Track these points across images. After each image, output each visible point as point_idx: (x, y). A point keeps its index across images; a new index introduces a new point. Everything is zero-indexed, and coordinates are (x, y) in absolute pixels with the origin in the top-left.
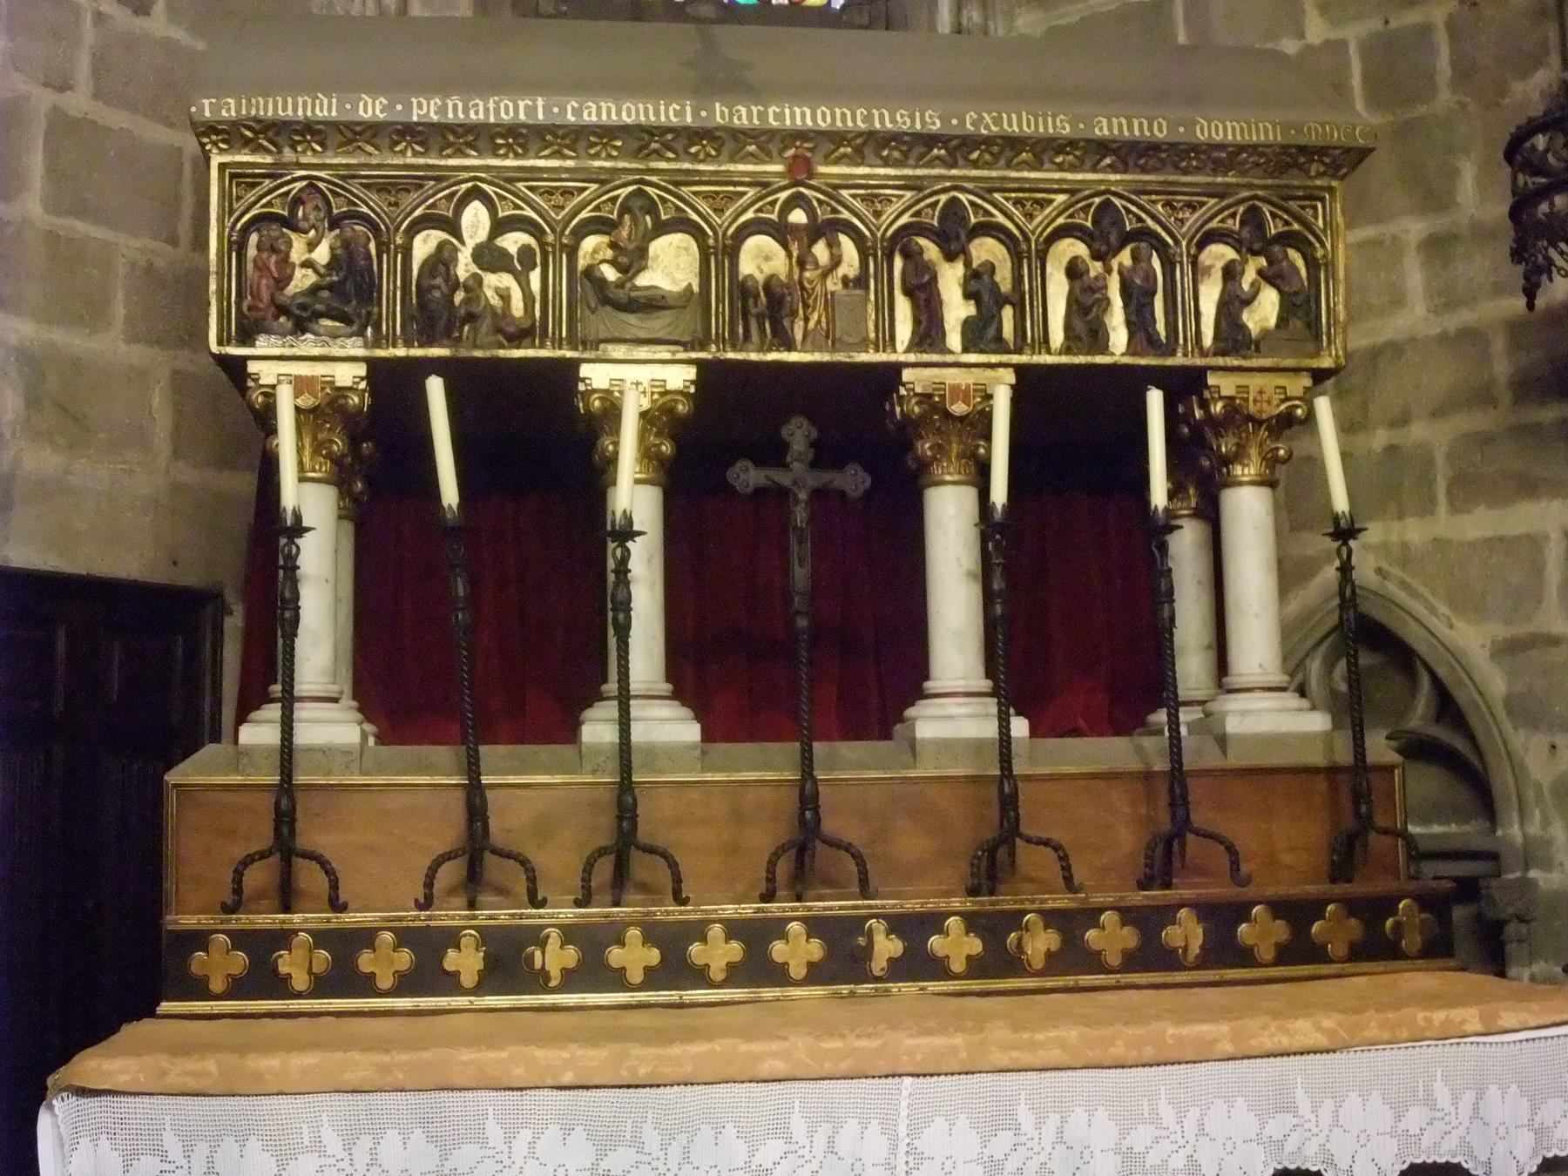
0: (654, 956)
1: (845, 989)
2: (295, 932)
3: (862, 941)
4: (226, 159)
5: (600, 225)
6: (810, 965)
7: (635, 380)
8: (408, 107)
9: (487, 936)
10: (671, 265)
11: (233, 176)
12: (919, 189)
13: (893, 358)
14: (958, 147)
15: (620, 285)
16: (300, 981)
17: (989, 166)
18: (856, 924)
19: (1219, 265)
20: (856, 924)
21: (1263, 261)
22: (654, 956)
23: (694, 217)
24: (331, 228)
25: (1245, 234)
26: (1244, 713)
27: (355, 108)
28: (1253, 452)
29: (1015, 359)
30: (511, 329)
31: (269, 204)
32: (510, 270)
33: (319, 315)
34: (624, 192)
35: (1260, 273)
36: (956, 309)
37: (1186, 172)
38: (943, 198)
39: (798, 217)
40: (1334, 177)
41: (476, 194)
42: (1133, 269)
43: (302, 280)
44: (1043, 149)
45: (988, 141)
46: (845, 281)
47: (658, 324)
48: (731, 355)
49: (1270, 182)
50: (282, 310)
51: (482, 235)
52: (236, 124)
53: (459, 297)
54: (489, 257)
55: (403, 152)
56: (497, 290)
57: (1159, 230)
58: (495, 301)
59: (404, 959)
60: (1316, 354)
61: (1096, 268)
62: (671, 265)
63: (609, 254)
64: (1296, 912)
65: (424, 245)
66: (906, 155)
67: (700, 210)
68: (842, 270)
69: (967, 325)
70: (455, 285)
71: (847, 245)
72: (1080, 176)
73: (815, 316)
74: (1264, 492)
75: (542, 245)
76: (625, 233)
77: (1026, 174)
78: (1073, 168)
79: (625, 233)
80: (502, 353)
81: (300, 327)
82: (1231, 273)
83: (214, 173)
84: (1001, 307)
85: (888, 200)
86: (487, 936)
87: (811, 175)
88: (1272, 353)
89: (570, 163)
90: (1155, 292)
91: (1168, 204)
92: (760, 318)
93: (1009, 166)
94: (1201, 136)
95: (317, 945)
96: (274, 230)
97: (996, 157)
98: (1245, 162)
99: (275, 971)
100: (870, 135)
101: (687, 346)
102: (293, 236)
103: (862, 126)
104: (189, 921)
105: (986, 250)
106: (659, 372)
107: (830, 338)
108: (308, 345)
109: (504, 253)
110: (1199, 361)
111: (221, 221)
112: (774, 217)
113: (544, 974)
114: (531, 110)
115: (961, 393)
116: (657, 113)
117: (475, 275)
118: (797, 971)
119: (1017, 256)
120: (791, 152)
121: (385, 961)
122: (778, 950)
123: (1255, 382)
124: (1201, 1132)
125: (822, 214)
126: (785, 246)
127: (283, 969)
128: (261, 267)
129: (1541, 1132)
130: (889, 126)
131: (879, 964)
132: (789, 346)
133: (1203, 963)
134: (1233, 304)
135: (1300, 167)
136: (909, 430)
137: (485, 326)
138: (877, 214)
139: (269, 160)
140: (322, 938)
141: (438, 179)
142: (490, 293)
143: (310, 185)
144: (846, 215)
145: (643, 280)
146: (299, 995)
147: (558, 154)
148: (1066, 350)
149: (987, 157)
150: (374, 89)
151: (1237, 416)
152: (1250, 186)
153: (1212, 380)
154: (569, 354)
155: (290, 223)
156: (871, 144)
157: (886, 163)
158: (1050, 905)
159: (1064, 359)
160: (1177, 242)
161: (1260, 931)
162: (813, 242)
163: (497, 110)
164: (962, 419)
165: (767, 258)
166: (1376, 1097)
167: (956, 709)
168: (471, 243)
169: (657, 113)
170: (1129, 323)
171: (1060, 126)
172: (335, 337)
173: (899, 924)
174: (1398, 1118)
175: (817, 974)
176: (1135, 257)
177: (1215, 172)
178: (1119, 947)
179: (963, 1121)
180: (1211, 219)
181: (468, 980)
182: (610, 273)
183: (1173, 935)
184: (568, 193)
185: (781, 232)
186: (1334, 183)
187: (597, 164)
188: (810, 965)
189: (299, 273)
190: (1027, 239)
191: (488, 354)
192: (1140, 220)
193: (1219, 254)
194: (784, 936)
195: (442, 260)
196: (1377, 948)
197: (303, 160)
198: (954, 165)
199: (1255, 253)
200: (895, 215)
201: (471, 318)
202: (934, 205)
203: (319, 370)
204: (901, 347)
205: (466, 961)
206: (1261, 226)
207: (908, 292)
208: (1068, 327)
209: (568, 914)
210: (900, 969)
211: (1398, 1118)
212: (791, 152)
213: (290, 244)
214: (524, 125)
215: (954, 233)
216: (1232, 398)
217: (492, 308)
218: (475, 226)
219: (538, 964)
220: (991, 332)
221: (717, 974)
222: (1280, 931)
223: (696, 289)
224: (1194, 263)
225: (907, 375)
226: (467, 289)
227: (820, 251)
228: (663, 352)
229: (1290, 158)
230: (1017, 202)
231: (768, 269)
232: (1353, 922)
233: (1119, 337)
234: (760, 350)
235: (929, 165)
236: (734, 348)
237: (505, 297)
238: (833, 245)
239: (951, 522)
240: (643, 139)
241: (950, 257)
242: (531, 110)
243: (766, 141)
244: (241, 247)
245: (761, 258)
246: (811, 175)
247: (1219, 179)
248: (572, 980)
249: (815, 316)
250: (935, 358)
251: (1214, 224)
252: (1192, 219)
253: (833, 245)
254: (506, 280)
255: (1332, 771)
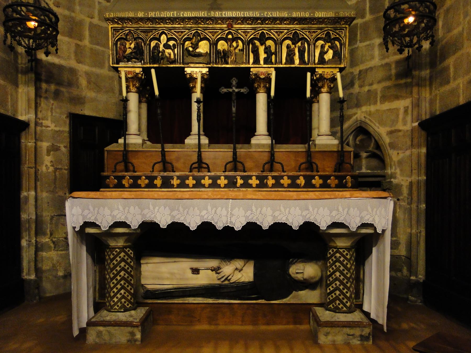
0: (194, 182)
1: (231, 189)
2: (126, 176)
3: (235, 180)
4: (112, 26)
5: (188, 39)
6: (225, 184)
7: (197, 71)
8: (148, 14)
9: (163, 177)
10: (203, 47)
11: (114, 30)
12: (255, 30)
13: (248, 66)
14: (263, 20)
15: (193, 51)
16: (127, 185)
17: (270, 24)
18: (235, 177)
19: (320, 45)
20: (235, 177)
21: (330, 44)
22: (194, 182)
23: (208, 37)
24: (134, 40)
25: (326, 38)
26: (320, 140)
27: (137, 14)
28: (326, 86)
29: (274, 66)
30: (170, 61)
31: (121, 35)
32: (171, 49)
33: (132, 58)
34: (193, 32)
35: (329, 46)
36: (262, 56)
37: (313, 24)
38: (260, 32)
39: (230, 37)
40: (347, 25)
41: (163, 33)
42: (300, 47)
43: (129, 51)
44: (282, 20)
45: (270, 18)
46: (239, 50)
47: (200, 59)
48: (215, 66)
49: (332, 26)
50: (125, 57)
51: (165, 42)
52: (113, 18)
53: (160, 54)
54: (167, 46)
55: (148, 24)
56: (168, 53)
57: (307, 38)
58: (168, 55)
59: (147, 181)
60: (340, 64)
61: (293, 46)
62: (203, 47)
63: (191, 45)
64: (325, 178)
65: (153, 44)
66: (252, 22)
67: (209, 36)
68: (239, 48)
69: (265, 59)
70: (159, 52)
71: (240, 42)
72: (290, 26)
73: (232, 58)
74: (328, 95)
75: (177, 43)
76: (194, 40)
77: (278, 26)
78: (288, 24)
79: (194, 40)
80: (169, 66)
81: (128, 61)
82: (323, 47)
83: (110, 29)
84: (272, 55)
85: (248, 32)
86: (163, 177)
87: (232, 27)
88: (331, 64)
89: (182, 26)
90: (305, 51)
91: (309, 32)
92: (222, 58)
93: (274, 24)
94: (316, 16)
95: (130, 179)
96: (123, 41)
97: (272, 22)
98: (326, 22)
99: (122, 184)
100: (244, 18)
101: (206, 64)
102: (127, 42)
103: (242, 16)
104: (105, 174)
105: (269, 43)
106: (201, 69)
107: (235, 62)
108: (130, 64)
109: (169, 45)
110: (314, 66)
111: (112, 39)
112: (225, 36)
113: (173, 185)
114: (173, 14)
115: (262, 73)
116: (199, 14)
117: (163, 50)
118: (222, 185)
119: (276, 44)
120: (227, 23)
121: (143, 182)
122: (219, 182)
123: (326, 70)
124: (289, 213)
125: (235, 36)
126: (227, 43)
127: (123, 183)
128: (120, 49)
129: (362, 218)
130: (248, 16)
131: (238, 185)
132: (227, 64)
133: (304, 187)
134: (323, 53)
135: (339, 22)
136: (254, 81)
137: (165, 60)
138: (246, 36)
139: (121, 26)
140: (131, 177)
141: (155, 30)
142: (166, 54)
143: (130, 32)
144: (240, 36)
145: (197, 50)
146: (127, 188)
147: (179, 24)
148: (285, 64)
149: (270, 22)
150: (141, 11)
151: (322, 78)
152: (327, 27)
153: (317, 70)
154: (182, 66)
155: (126, 39)
156: (244, 20)
157: (248, 24)
158: (273, 175)
159: (285, 66)
160: (311, 40)
161: (317, 181)
162: (232, 43)
163: (166, 14)
164: (263, 79)
165: (223, 46)
166: (326, 209)
167: (261, 138)
168: (163, 43)
169: (199, 14)
170: (299, 58)
171: (285, 14)
172: (135, 62)
173: (242, 177)
174: (331, 213)
175: (226, 186)
176: (302, 44)
177: (320, 24)
178: (287, 183)
179: (241, 209)
180: (318, 35)
181: (159, 186)
182: (191, 49)
183: (298, 182)
184: (182, 32)
185: (226, 40)
186: (347, 26)
187: (188, 26)
188: (225, 184)
189: (128, 50)
190: (278, 40)
191: (166, 66)
192: (303, 35)
193: (321, 42)
194: (220, 179)
195: (157, 46)
196: (341, 186)
197: (128, 26)
198: (263, 24)
199: (328, 42)
200: (250, 36)
201: (163, 59)
202: (258, 33)
203: (132, 70)
204: (251, 64)
205: (158, 182)
206: (330, 36)
207: (252, 52)
208: (286, 59)
209: (177, 174)
210: (242, 186)
211: (331, 213)
212: (227, 23)
213: (126, 44)
214: (172, 18)
215: (263, 39)
216: (321, 74)
217: (167, 57)
218: (164, 40)
219: (172, 183)
220: (269, 60)
221: (207, 186)
222: (321, 181)
223: (208, 52)
224: (314, 44)
225: (252, 70)
226: (162, 53)
227: (234, 44)
228: (201, 65)
229: (336, 20)
230: (276, 32)
231: (223, 48)
232: (337, 181)
233: (297, 61)
234: (221, 65)
235: (257, 24)
236: (216, 64)
237: (170, 54)
238: (237, 42)
239: (261, 100)
240: (196, 20)
241: (262, 45)
242: (173, 14)
243: (223, 20)
244: (116, 44)
245: (222, 46)
246: (232, 27)
247: (321, 26)
248: (179, 186)
249: (232, 58)
250: (257, 66)
251: (319, 36)
252: (314, 35)
253: (237, 42)
254: (170, 51)
255: (338, 152)
